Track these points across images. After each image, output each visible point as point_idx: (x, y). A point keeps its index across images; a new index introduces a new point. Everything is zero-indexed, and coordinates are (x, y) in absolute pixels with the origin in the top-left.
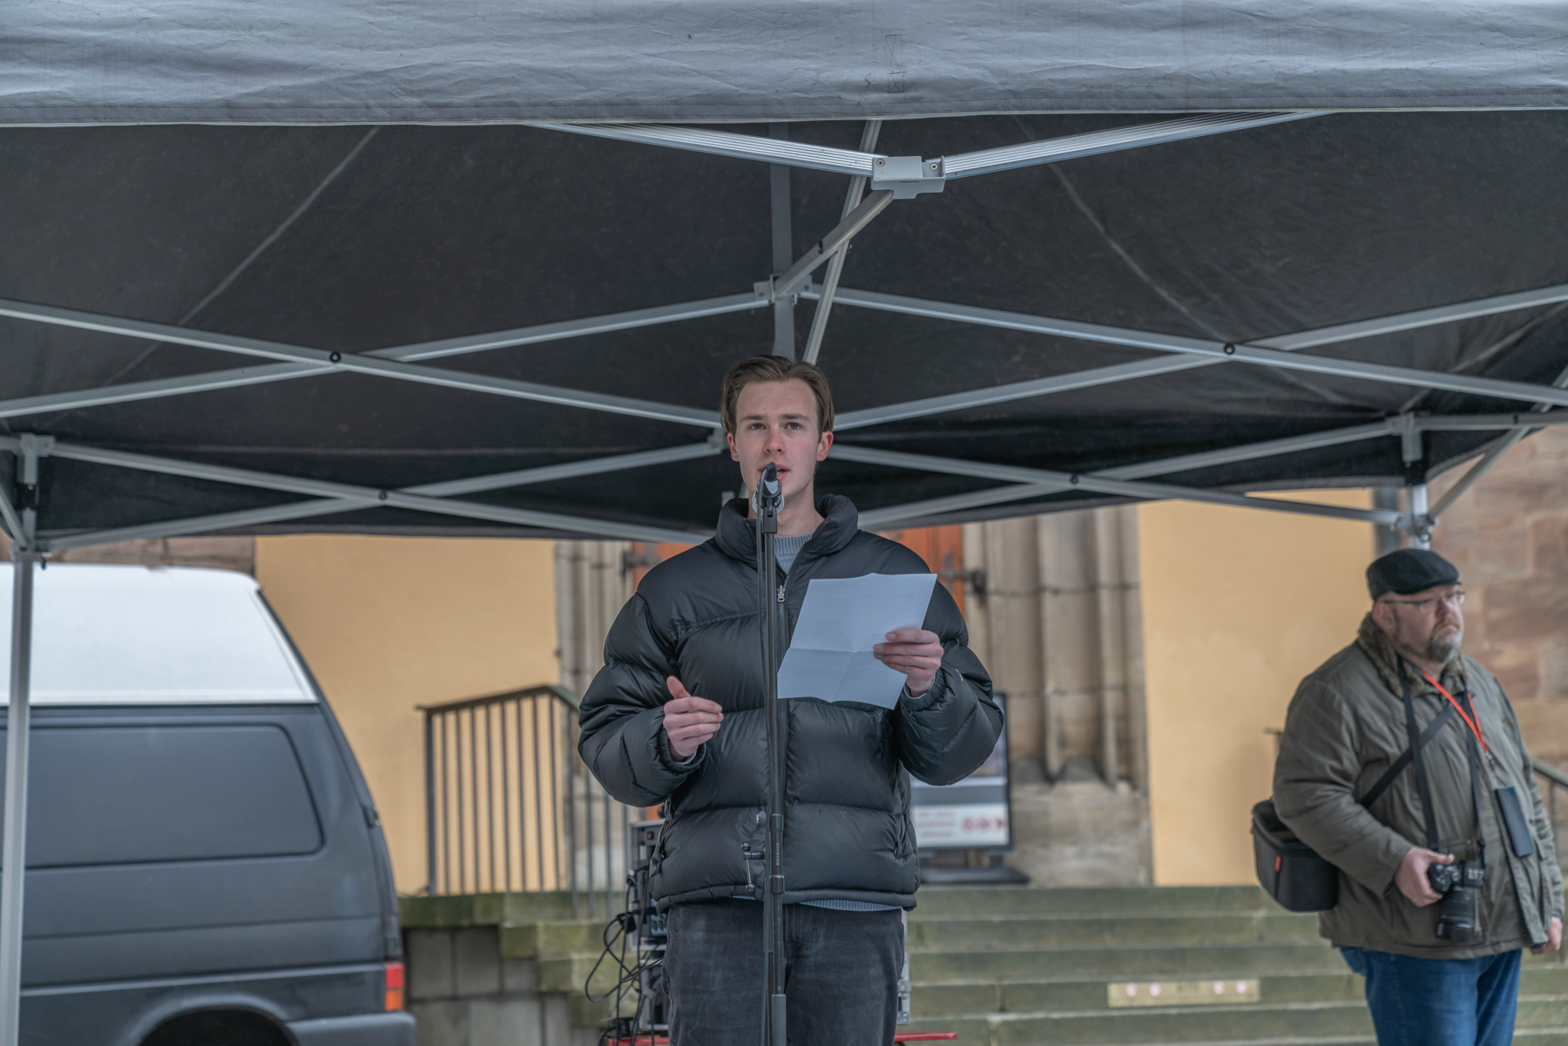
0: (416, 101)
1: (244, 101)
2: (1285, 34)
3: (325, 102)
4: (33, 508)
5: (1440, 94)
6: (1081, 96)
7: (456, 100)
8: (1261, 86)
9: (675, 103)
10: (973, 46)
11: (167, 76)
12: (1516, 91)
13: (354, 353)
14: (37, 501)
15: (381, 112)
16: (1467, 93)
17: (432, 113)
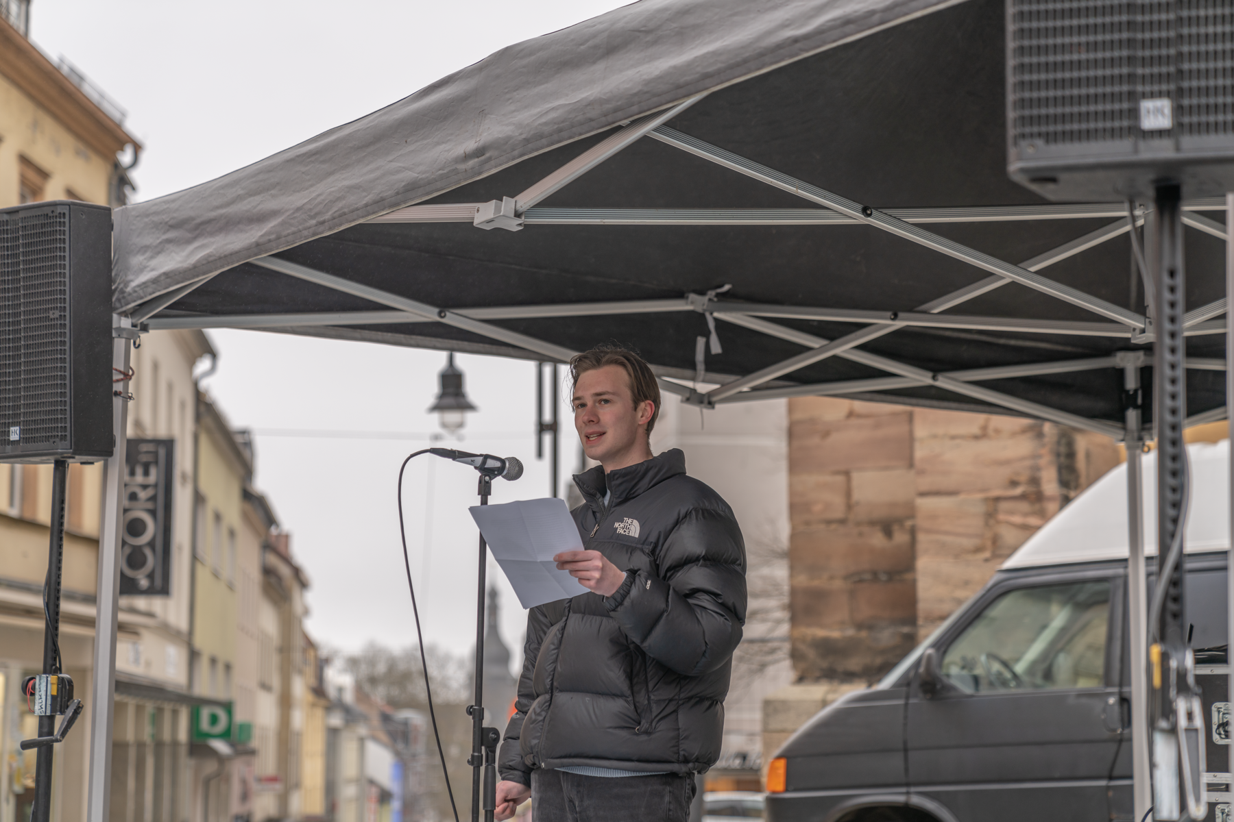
0: (314, 222)
1: (261, 241)
2: (655, 42)
3: (286, 233)
4: (1136, 407)
5: (731, 67)
6: (560, 130)
7: (327, 216)
8: (635, 94)
9: (398, 193)
10: (512, 107)
11: (242, 231)
12: (779, 46)
13: (911, 310)
14: (1139, 401)
15: (305, 233)
16: (745, 61)
17: (321, 228)
